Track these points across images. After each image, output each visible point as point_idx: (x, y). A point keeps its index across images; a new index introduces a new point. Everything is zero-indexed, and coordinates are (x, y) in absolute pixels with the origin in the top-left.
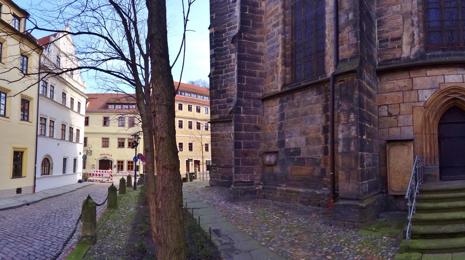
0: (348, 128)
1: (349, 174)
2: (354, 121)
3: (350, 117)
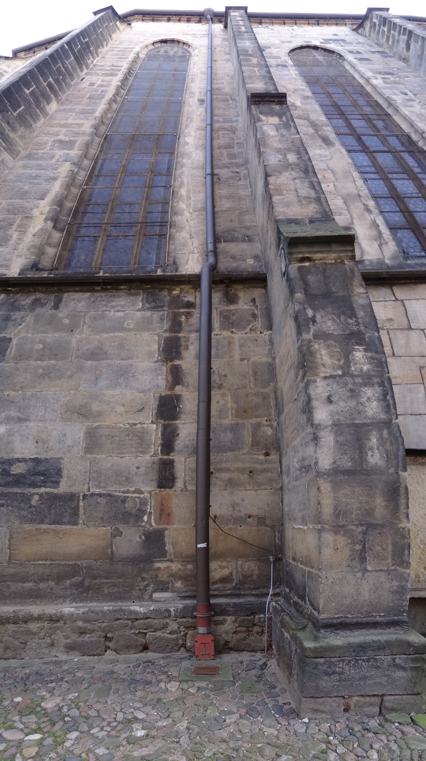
0: (352, 391)
1: (364, 547)
2: (368, 370)
3: (351, 357)
